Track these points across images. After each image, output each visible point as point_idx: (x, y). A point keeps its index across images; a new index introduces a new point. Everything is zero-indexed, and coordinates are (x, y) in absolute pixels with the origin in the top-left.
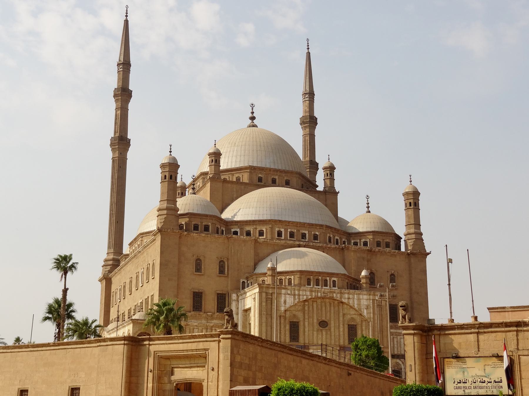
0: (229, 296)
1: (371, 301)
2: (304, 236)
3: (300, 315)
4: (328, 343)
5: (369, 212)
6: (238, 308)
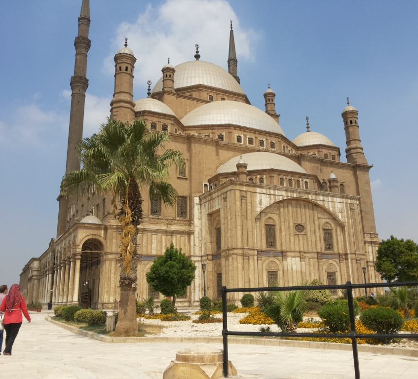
0: (191, 200)
1: (345, 204)
2: (262, 143)
3: (275, 217)
4: (306, 251)
5: (309, 131)
6: (201, 213)
